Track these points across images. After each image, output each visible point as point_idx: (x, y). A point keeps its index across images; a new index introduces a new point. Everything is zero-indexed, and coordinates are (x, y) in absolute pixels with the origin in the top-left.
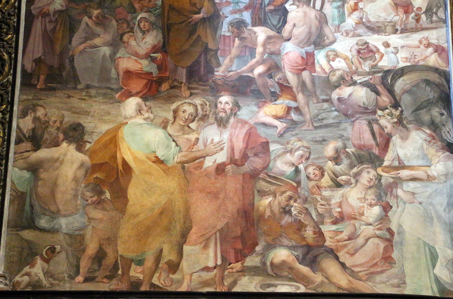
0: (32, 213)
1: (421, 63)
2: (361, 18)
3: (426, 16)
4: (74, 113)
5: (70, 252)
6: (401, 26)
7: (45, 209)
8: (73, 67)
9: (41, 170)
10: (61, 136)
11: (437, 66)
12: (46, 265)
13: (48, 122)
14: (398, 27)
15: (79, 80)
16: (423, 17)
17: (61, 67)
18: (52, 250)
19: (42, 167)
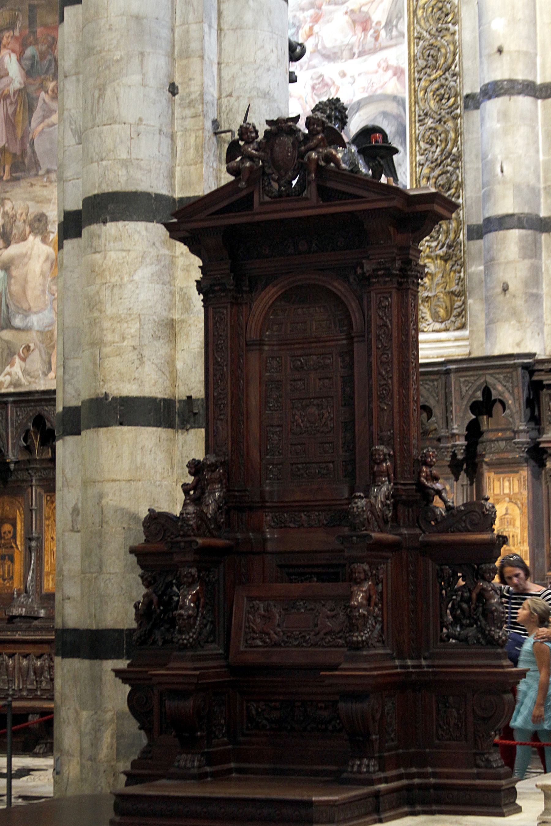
0: (8, 313)
1: (379, 92)
2: (317, 45)
3: (386, 31)
4: (38, 202)
5: (42, 349)
6: (358, 48)
7: (18, 308)
8: (34, 152)
9: (13, 268)
10: (28, 229)
11: (395, 93)
12: (23, 364)
13: (16, 216)
14: (356, 51)
15: (40, 166)
16: (383, 33)
17: (23, 152)
18: (28, 348)
19: (13, 264)
